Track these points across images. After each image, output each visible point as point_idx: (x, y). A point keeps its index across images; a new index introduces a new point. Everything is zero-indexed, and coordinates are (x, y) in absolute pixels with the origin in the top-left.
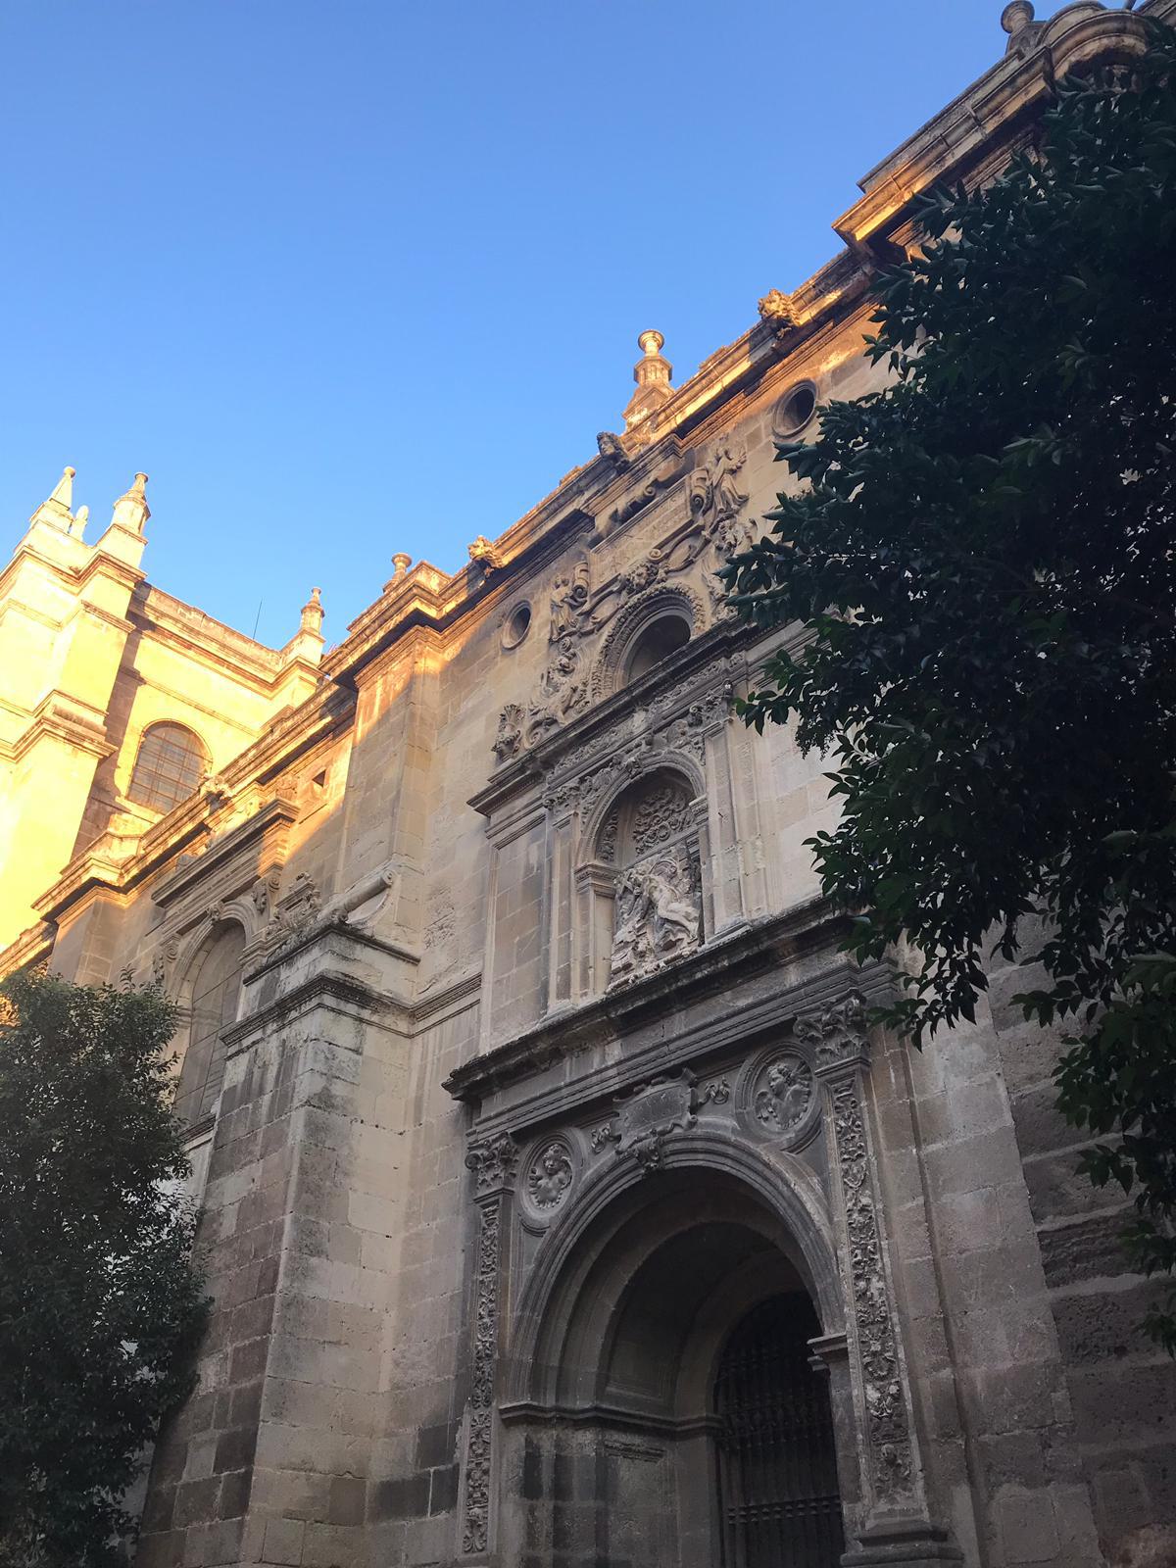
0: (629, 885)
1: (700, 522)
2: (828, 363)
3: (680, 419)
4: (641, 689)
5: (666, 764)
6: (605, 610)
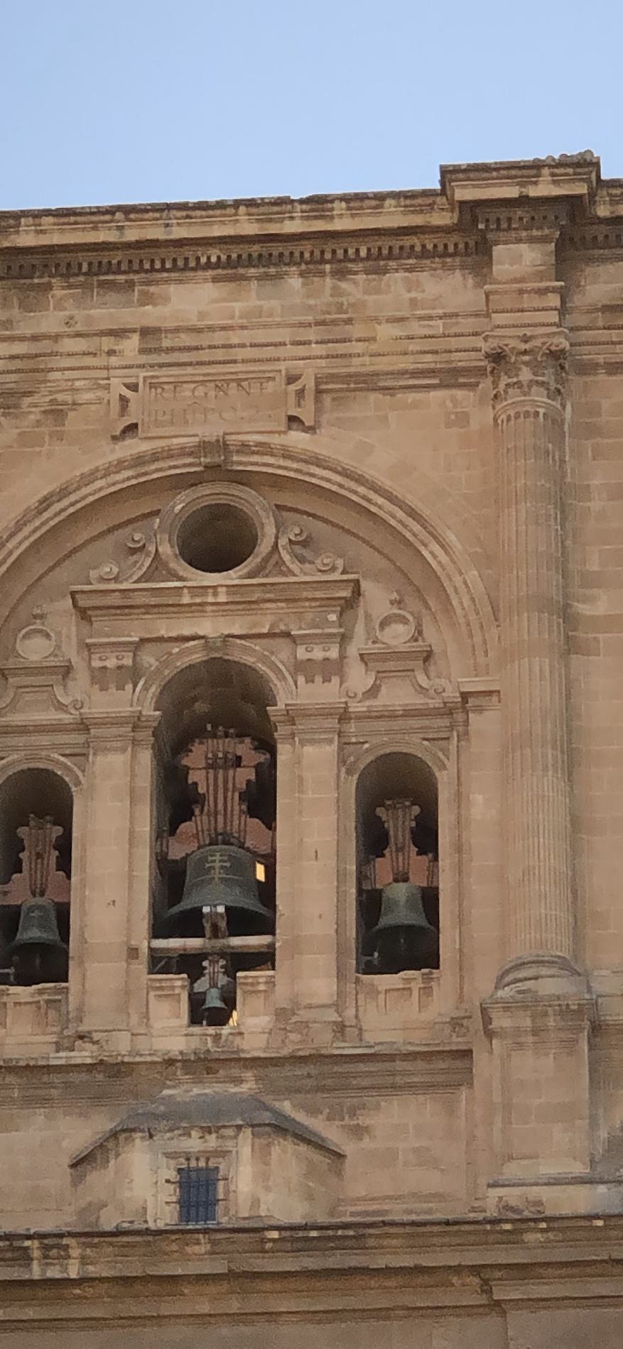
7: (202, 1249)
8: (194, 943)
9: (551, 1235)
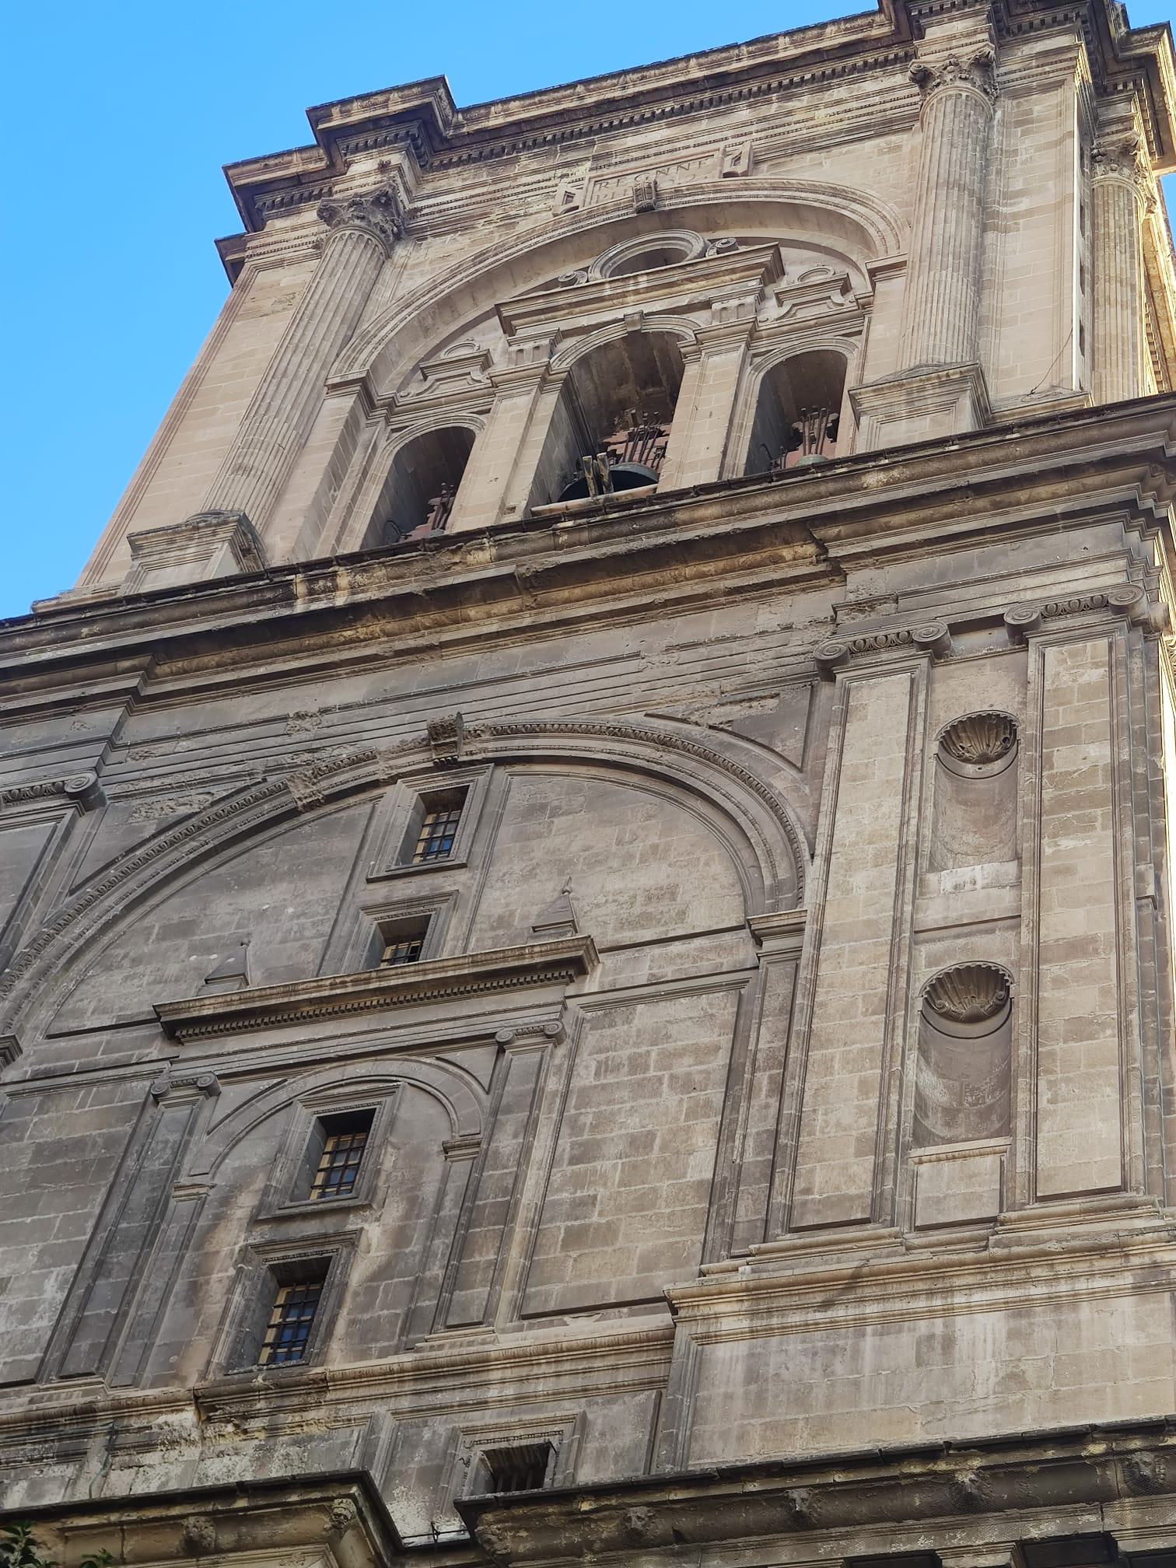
9: (895, 473)
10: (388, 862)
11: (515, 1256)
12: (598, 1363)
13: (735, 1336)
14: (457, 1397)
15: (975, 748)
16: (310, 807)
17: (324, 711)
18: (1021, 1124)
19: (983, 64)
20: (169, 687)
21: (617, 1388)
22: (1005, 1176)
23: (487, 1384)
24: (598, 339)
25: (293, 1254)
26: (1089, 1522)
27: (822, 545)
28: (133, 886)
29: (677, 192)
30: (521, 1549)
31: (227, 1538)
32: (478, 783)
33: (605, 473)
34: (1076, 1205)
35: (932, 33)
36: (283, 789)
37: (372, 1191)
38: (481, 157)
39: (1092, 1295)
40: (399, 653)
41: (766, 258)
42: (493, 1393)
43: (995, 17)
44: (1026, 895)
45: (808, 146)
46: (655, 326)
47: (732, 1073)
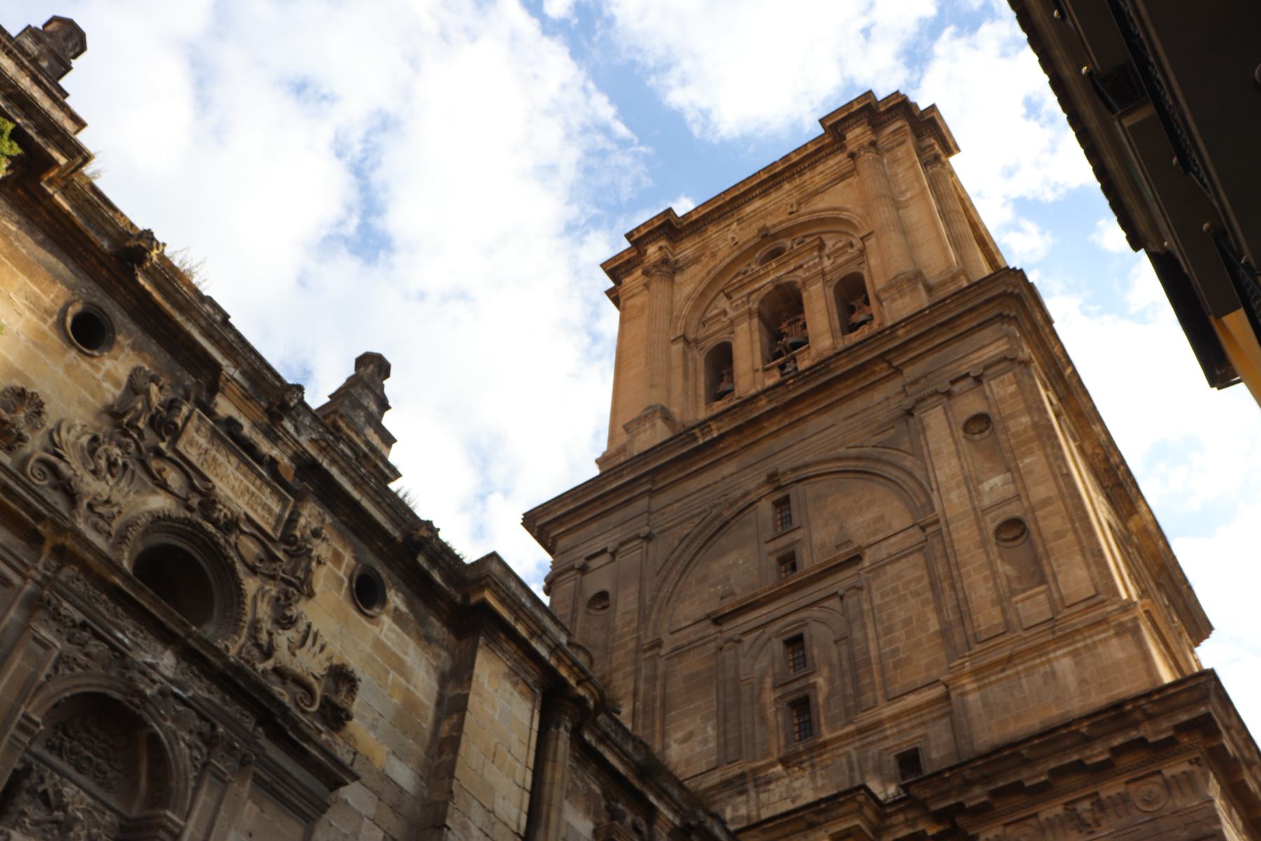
0: (52, 797)
1: (280, 555)
2: (397, 595)
3: (325, 464)
4: (197, 647)
5: (162, 735)
6: (173, 478)
7: (763, 402)
8: (780, 360)
9: (909, 327)
10: (769, 534)
11: (877, 677)
12: (924, 712)
13: (973, 690)
14: (876, 737)
15: (975, 428)
16: (732, 518)
17: (724, 478)
18: (1050, 579)
19: (873, 144)
20: (661, 484)
21: (934, 719)
22: (1051, 600)
23: (885, 730)
24: (764, 292)
25: (794, 697)
26: (1134, 734)
27: (890, 363)
28: (679, 567)
29: (774, 226)
30: (928, 795)
31: (822, 819)
32: (792, 492)
33: (788, 346)
34: (1082, 606)
35: (850, 136)
36: (719, 515)
37: (814, 665)
38: (694, 232)
39: (1101, 641)
40: (743, 448)
41: (817, 242)
42: (889, 732)
43: (870, 123)
44: (1019, 486)
45: (817, 192)
46: (785, 280)
47: (933, 585)
